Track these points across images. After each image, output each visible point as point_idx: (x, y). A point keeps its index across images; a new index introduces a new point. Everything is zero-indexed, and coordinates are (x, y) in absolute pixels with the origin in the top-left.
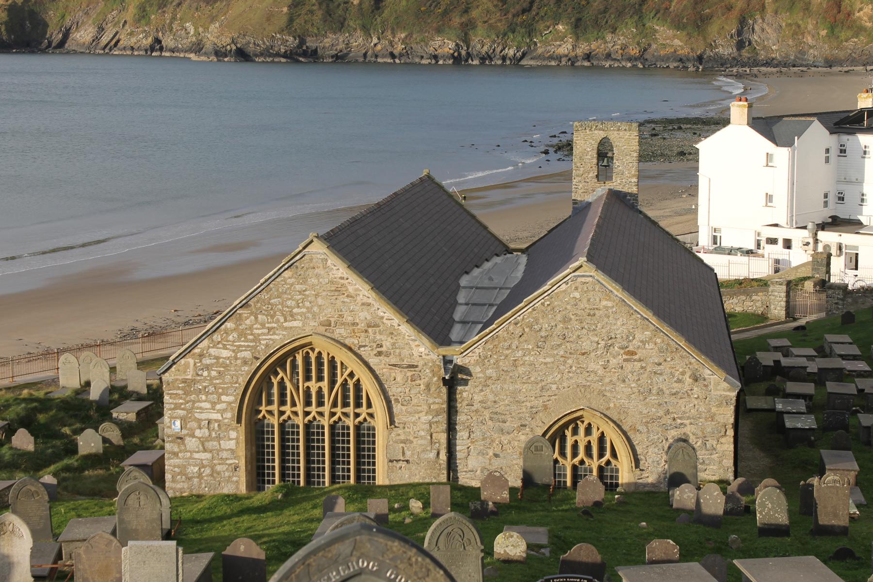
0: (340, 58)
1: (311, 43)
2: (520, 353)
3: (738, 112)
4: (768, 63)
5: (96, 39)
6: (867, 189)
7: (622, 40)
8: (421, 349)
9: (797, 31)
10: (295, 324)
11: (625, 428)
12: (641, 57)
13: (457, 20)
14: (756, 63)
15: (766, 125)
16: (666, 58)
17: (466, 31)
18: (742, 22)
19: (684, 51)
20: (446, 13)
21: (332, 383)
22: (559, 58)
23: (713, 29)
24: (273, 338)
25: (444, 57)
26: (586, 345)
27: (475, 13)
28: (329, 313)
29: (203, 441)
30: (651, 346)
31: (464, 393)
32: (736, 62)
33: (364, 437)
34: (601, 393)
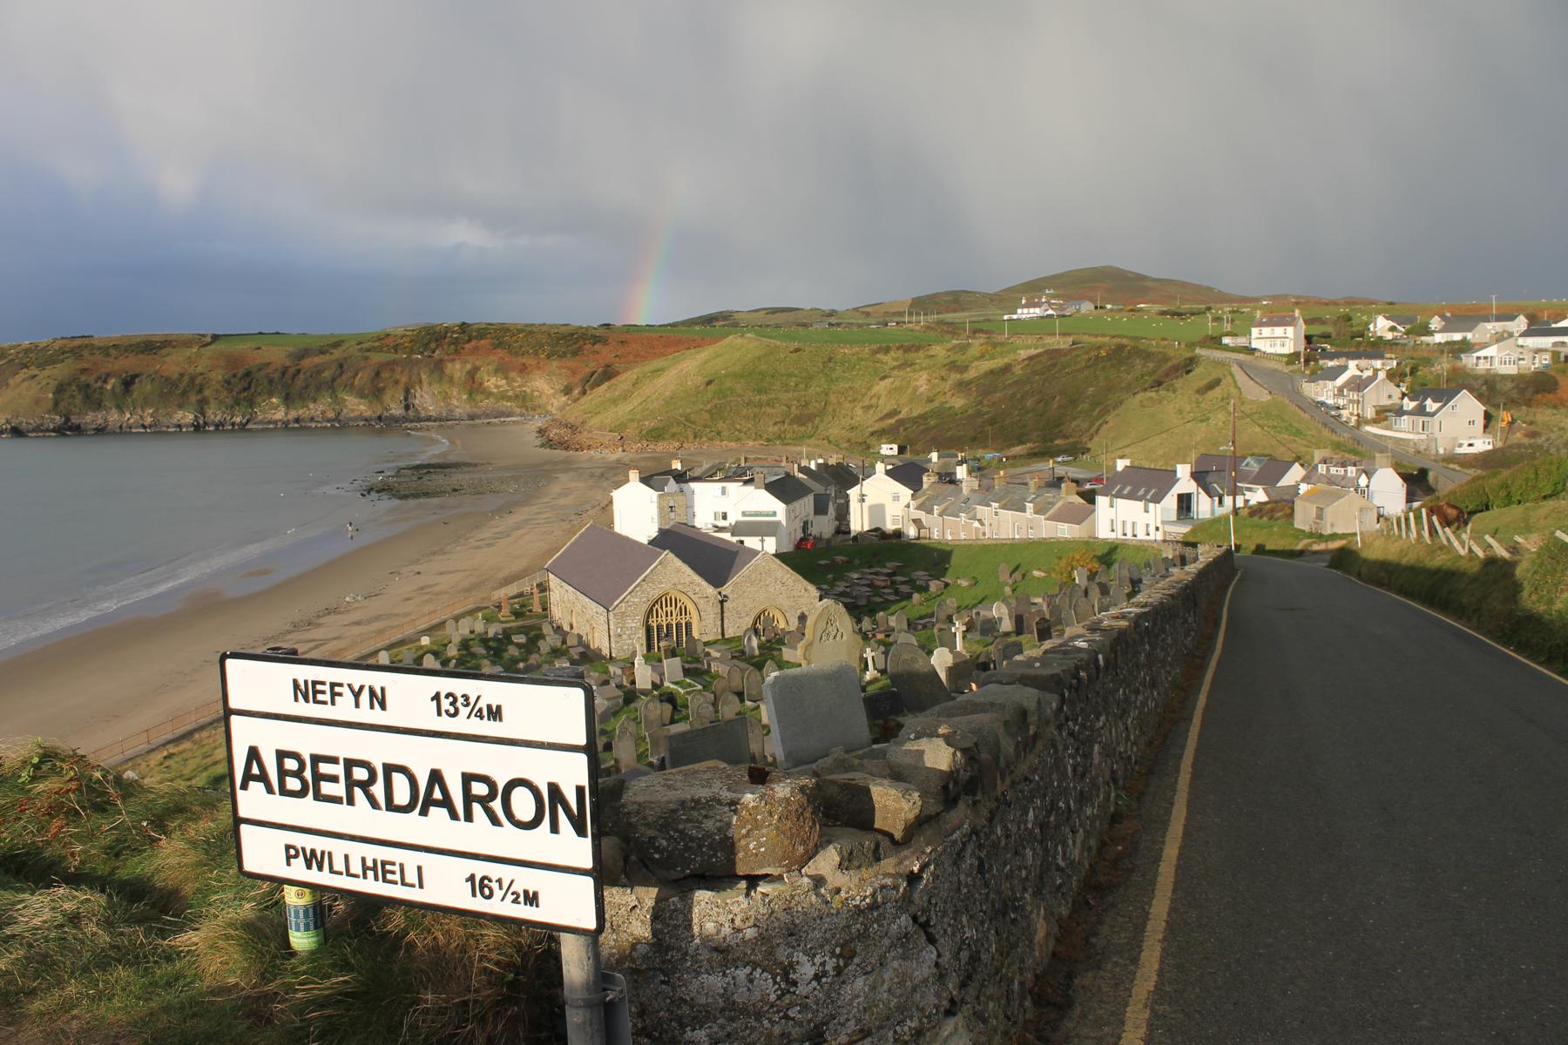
0: (101, 431)
1: (75, 420)
3: (634, 475)
4: (429, 419)
6: (697, 509)
7: (321, 408)
8: (711, 590)
9: (446, 397)
12: (337, 419)
13: (193, 398)
14: (420, 420)
15: (645, 480)
16: (355, 419)
17: (201, 406)
18: (407, 391)
19: (368, 414)
20: (184, 393)
22: (275, 422)
23: (387, 397)
24: (656, 594)
25: (187, 426)
27: (207, 393)
28: (675, 580)
32: (406, 419)
33: (688, 625)
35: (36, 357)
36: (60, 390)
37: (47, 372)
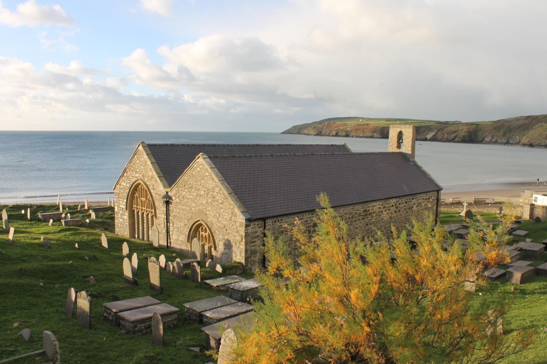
2: (184, 193)
10: (137, 175)
11: (212, 231)
21: (146, 198)
26: (202, 193)
29: (122, 215)
30: (219, 195)
31: (171, 207)
34: (206, 214)
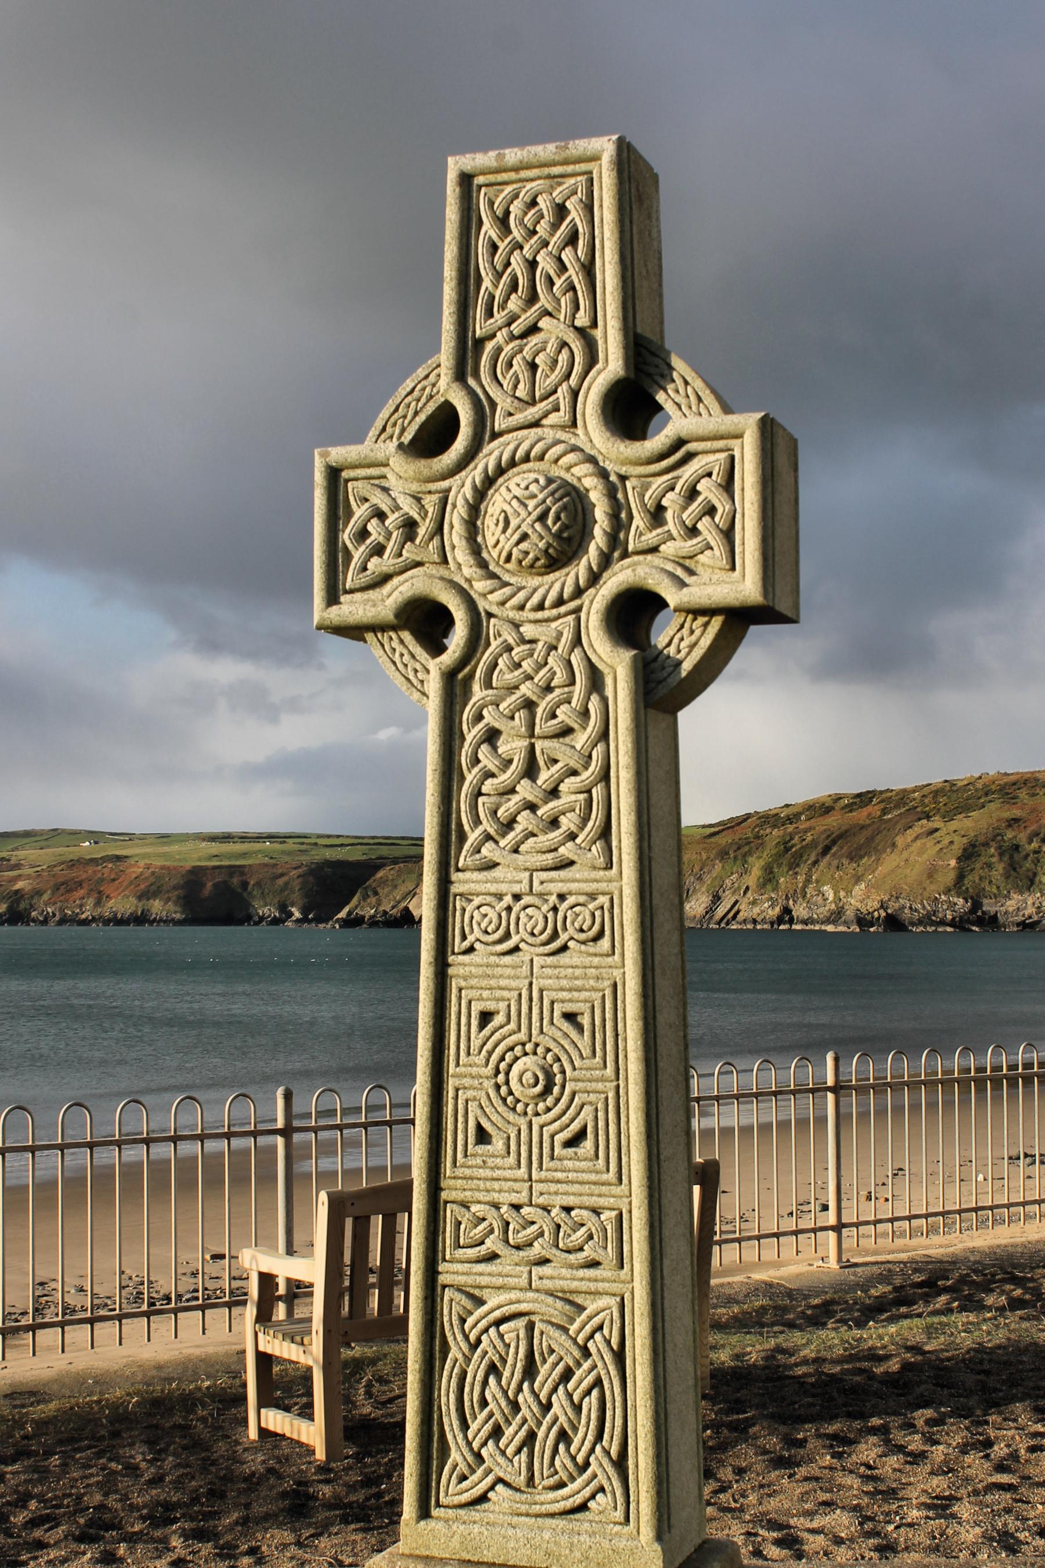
1: (989, 906)
5: (710, 910)
35: (951, 799)
36: (969, 854)
37: (954, 825)
